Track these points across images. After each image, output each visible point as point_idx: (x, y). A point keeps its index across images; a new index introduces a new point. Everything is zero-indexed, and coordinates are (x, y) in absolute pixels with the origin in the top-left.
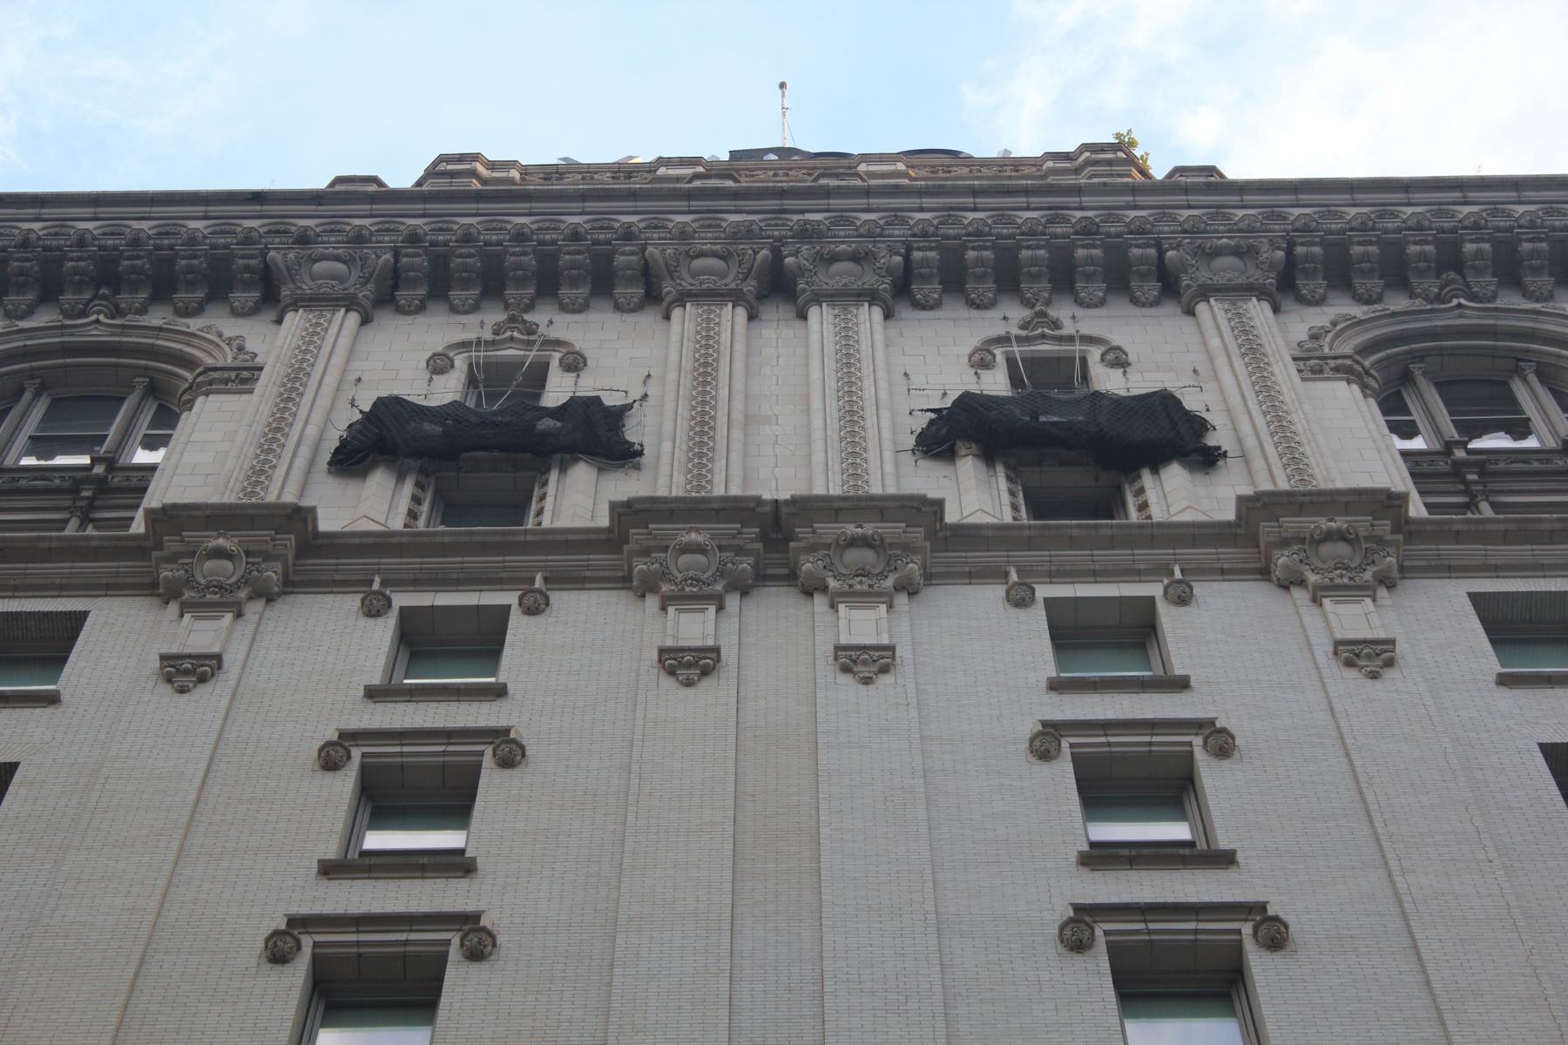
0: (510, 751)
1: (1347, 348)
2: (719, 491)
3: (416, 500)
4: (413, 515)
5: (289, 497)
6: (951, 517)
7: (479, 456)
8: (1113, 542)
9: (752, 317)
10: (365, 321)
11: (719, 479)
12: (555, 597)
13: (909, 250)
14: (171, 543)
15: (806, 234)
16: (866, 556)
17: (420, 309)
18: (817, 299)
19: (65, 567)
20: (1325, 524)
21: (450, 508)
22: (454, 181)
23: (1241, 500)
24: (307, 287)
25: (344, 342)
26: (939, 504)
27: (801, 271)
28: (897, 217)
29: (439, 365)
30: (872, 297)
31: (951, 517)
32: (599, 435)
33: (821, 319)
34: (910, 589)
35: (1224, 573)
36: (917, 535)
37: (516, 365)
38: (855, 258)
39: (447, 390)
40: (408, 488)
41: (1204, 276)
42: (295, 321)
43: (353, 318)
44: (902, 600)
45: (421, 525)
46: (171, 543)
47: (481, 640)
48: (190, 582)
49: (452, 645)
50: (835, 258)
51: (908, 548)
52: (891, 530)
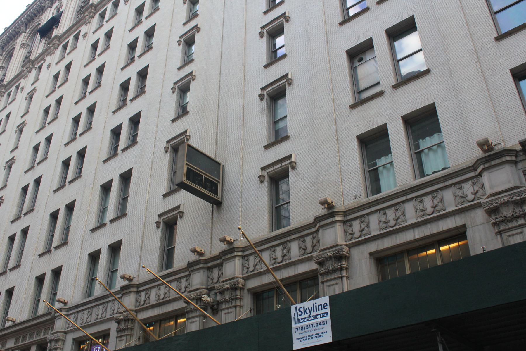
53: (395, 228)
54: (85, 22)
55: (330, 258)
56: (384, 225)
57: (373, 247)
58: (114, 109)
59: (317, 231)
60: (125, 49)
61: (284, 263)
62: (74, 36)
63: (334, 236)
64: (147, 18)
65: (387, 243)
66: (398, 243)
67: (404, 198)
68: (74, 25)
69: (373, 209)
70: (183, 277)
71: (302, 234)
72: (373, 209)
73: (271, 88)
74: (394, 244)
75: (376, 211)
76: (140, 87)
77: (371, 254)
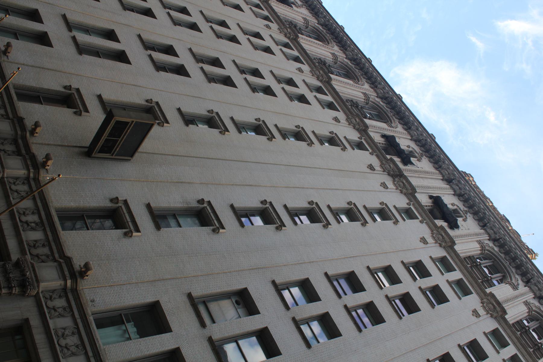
0: (396, 222)
1: (534, 309)
2: (504, 306)
3: (429, 206)
4: (426, 206)
5: (456, 242)
6: (506, 317)
7: (438, 209)
8: (481, 289)
9: (534, 298)
10: (454, 195)
11: (506, 305)
12: (424, 224)
13: (501, 238)
14: (440, 230)
15: (459, 181)
16: (441, 238)
17: (461, 201)
18: (529, 287)
19: (345, 109)
20: (443, 234)
21: (431, 211)
22: (464, 175)
23: (441, 225)
24: (442, 171)
25: (448, 193)
26: (455, 244)
27: (453, 183)
28: (494, 222)
29: (453, 204)
30: (535, 294)
31: (506, 317)
32: (454, 225)
33: (527, 289)
34: (492, 316)
35: (429, 227)
36: (500, 313)
37: (459, 213)
38: (494, 232)
39: (450, 206)
40: (430, 204)
41: (488, 230)
42: (482, 231)
43: (488, 238)
44: (489, 315)
45: (425, 208)
46: (440, 230)
47: (466, 292)
48: (350, 119)
49: (409, 214)
50: (537, 286)
51: (497, 312)
52: (448, 240)
53: (57, 346)
54: (282, 28)
55: (24, 275)
56: (60, 334)
57: (35, 322)
58: (194, 50)
59: (55, 260)
60: (254, 66)
61: (19, 224)
62: (268, 16)
63: (49, 278)
64: (283, 89)
65: (39, 338)
66: (39, 350)
67: (90, 354)
68: (278, 17)
69: (79, 321)
70: (6, 111)
71: (53, 244)
72: (79, 321)
73: (210, 211)
74: (38, 346)
75: (76, 323)
76: (215, 77)
77: (27, 320)
